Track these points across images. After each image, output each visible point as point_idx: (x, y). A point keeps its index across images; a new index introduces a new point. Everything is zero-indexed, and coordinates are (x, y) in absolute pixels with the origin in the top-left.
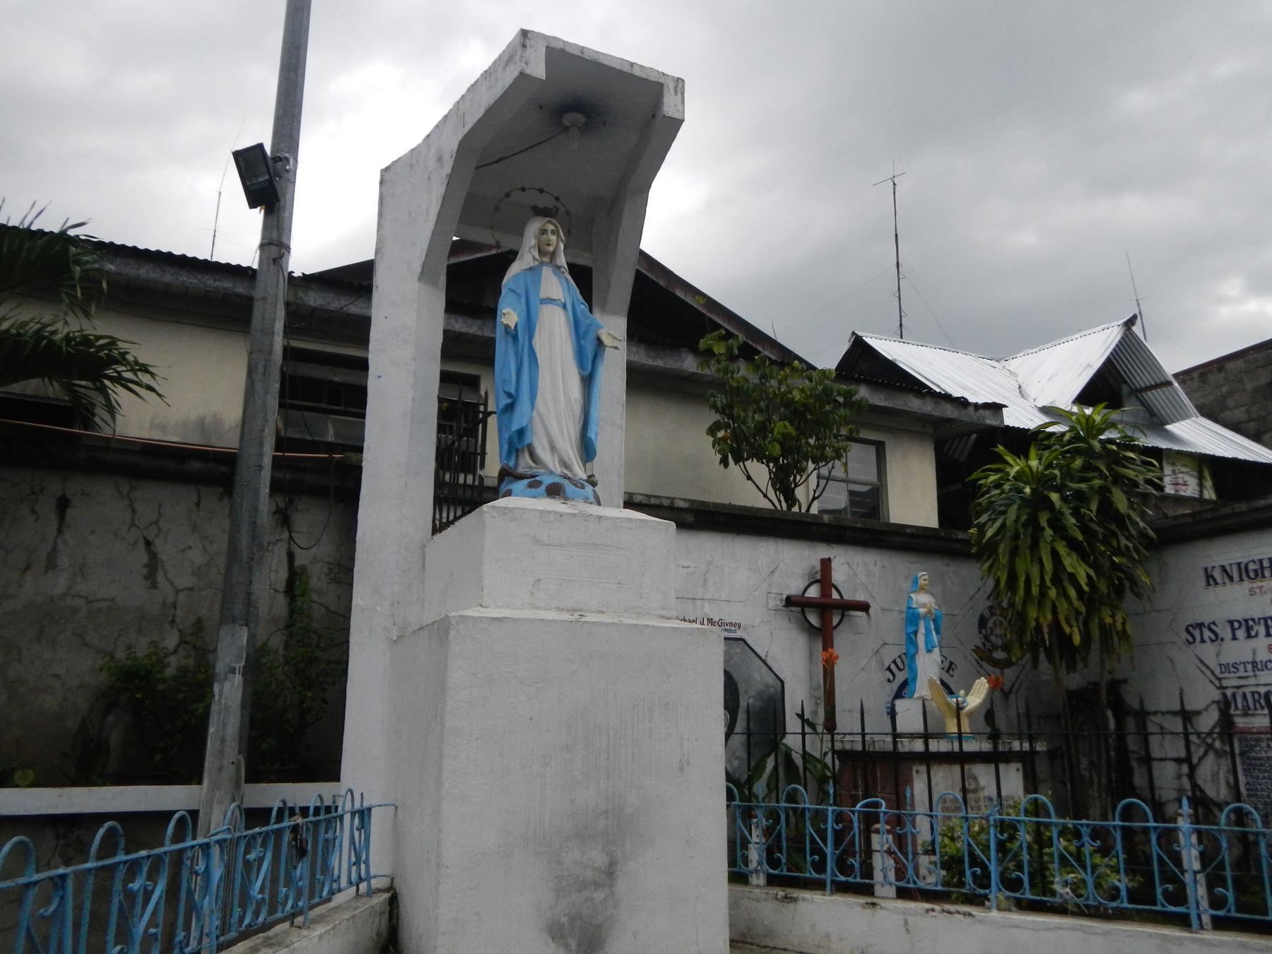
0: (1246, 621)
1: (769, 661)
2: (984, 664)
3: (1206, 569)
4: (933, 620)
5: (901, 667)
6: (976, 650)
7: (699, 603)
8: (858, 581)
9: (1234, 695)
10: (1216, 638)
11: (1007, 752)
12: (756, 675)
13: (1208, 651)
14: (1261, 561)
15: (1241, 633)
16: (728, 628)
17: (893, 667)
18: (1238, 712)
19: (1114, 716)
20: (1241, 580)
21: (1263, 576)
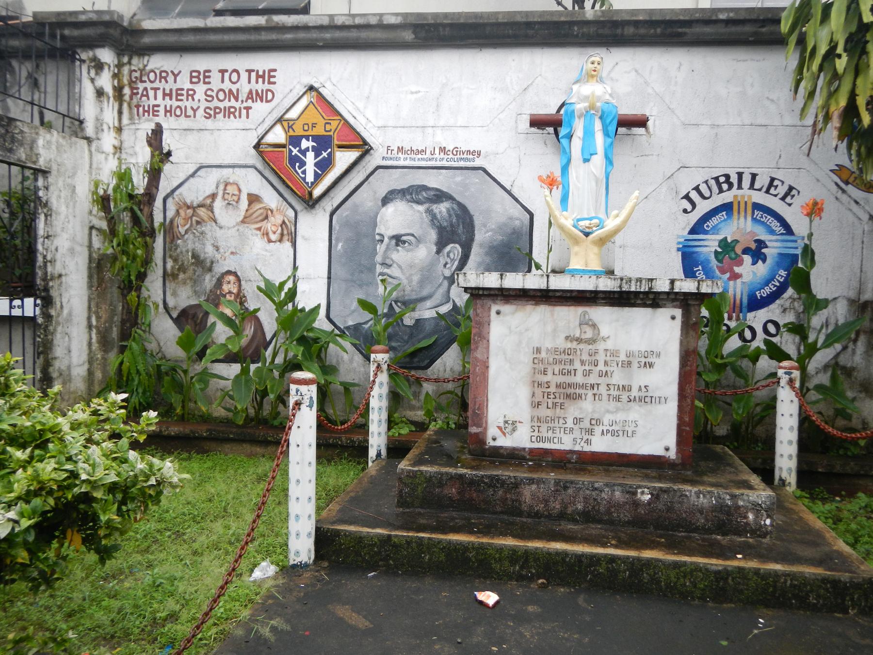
1: (515, 192)
2: (850, 189)
4: (601, 118)
5: (707, 194)
6: (839, 171)
7: (430, 130)
8: (650, 91)
11: (645, 293)
12: (498, 208)
16: (465, 156)
17: (694, 195)
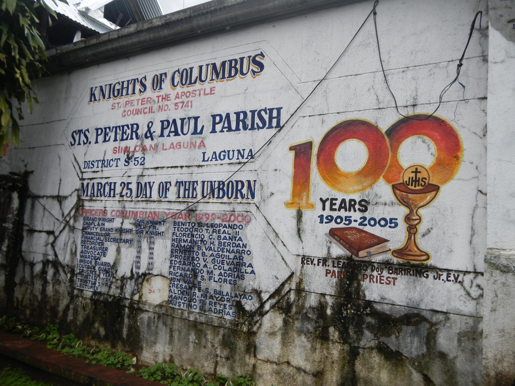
0: (105, 129)
3: (92, 88)
9: (88, 184)
10: (87, 142)
13: (80, 151)
14: (123, 82)
15: (101, 138)
18: (88, 198)
19: (19, 197)
20: (109, 97)
21: (122, 95)
